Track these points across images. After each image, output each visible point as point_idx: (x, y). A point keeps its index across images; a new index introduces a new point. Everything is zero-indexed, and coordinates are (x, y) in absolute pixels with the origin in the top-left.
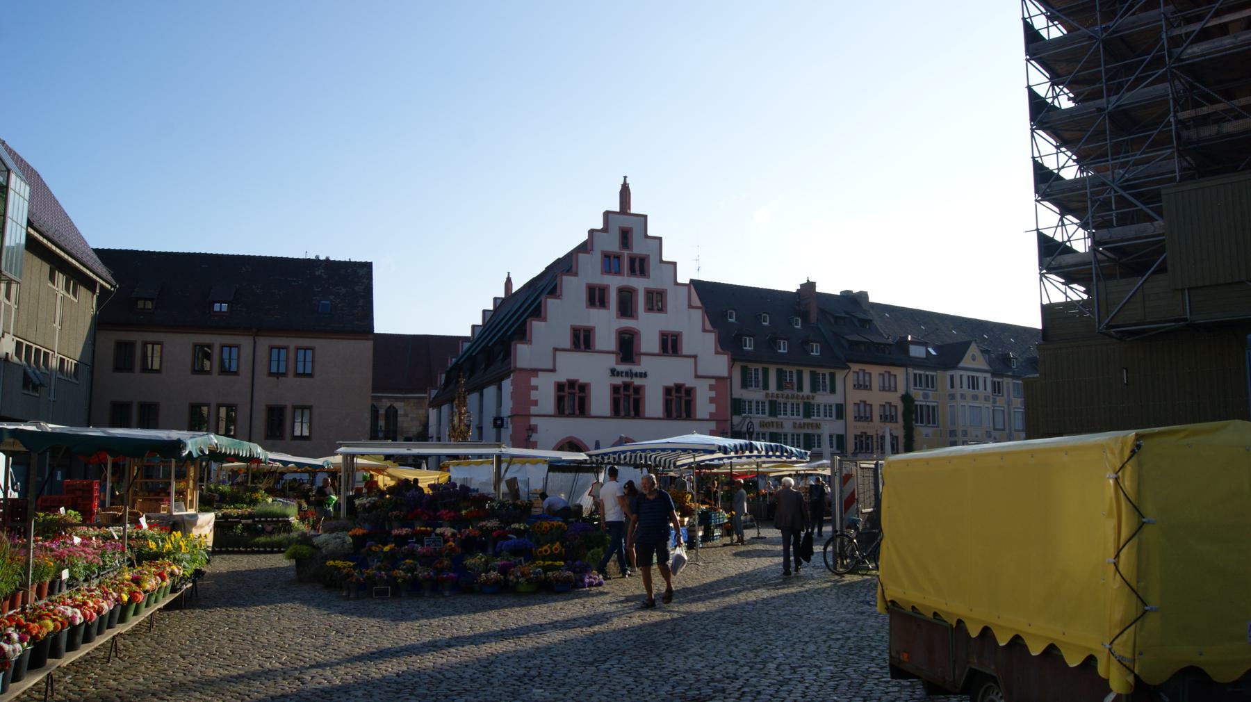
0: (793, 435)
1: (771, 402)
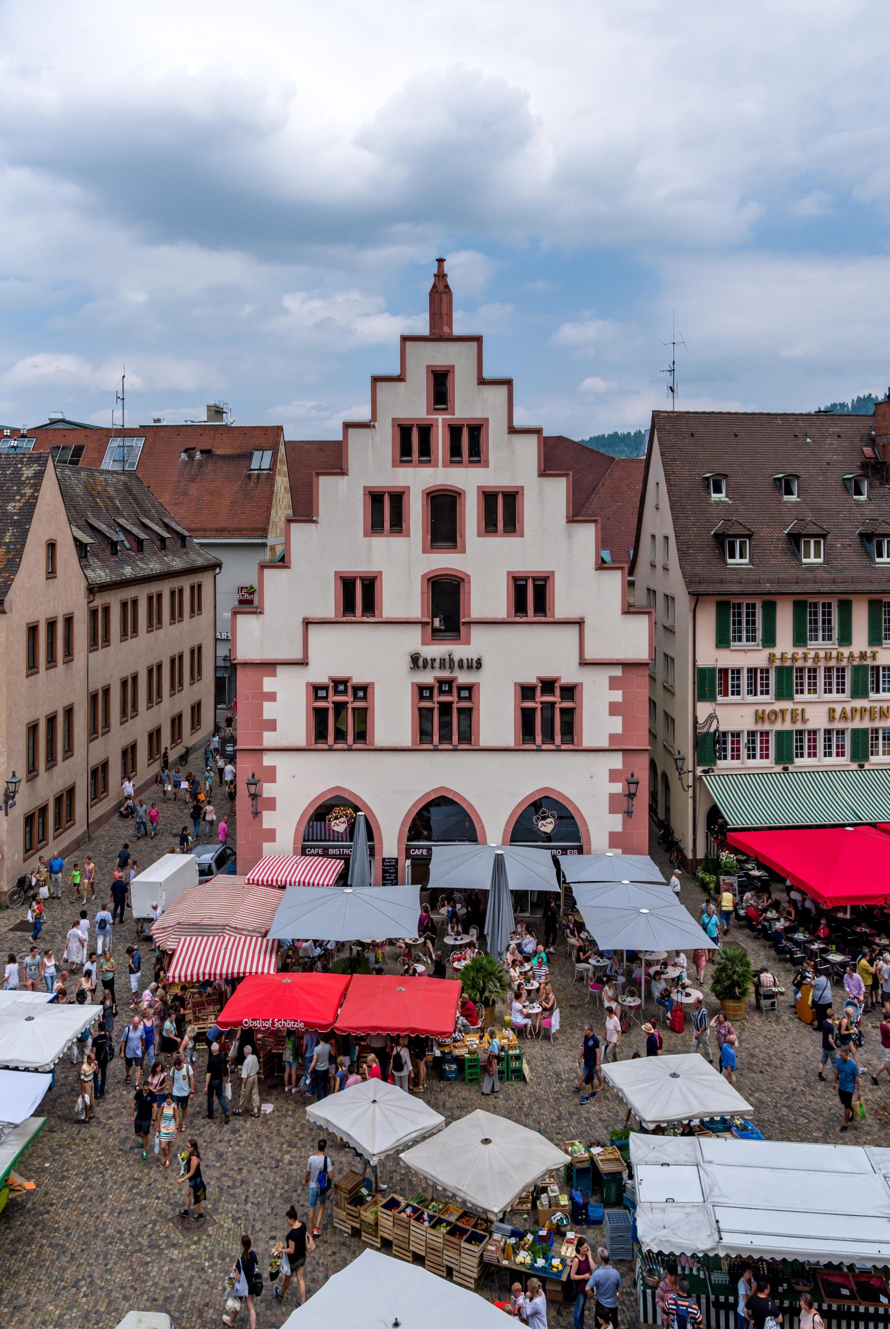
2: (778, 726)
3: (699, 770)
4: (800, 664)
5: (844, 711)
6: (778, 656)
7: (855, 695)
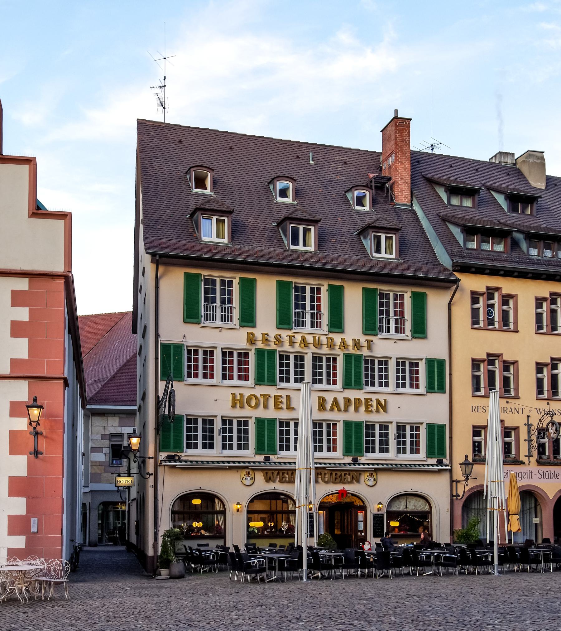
1: (260, 353)
2: (261, 413)
3: (162, 456)
4: (287, 347)
5: (335, 401)
7: (347, 385)
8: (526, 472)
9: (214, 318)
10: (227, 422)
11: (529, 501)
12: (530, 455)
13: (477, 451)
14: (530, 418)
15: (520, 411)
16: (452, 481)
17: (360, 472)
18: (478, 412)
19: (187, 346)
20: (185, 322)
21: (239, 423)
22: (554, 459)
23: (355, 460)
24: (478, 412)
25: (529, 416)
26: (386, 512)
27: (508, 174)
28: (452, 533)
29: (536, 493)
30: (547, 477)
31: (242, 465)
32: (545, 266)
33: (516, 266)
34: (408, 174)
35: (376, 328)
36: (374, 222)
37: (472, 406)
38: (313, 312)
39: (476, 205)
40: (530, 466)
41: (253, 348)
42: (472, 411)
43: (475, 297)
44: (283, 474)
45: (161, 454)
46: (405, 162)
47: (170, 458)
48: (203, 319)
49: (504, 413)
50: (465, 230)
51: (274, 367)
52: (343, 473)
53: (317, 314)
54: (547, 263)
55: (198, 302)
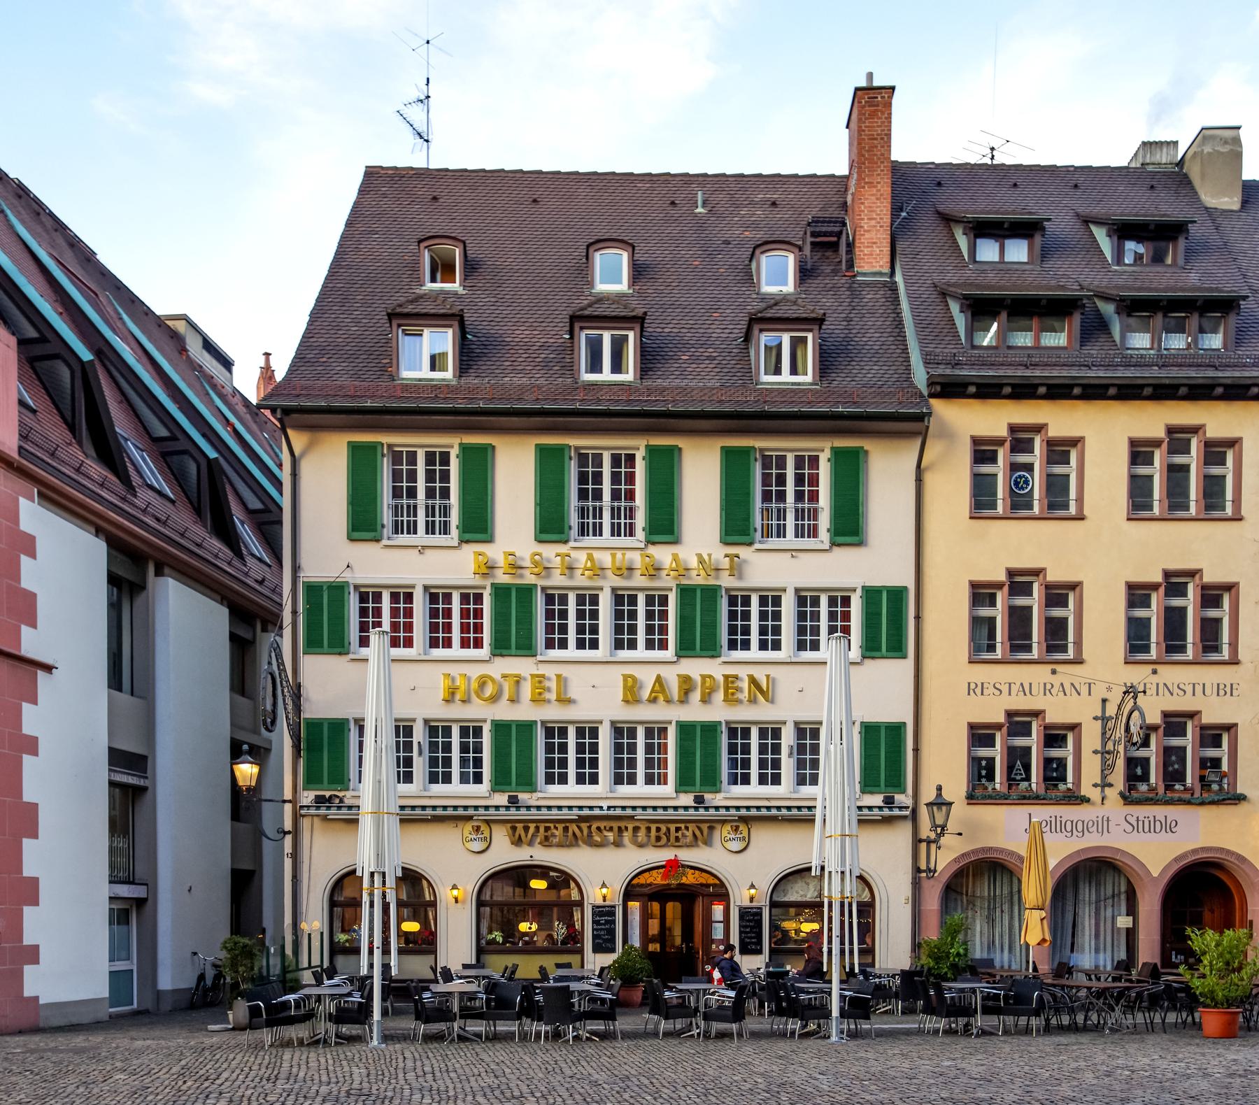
0: (617, 730)
2: (505, 712)
3: (308, 797)
4: (557, 580)
6: (501, 561)
7: (686, 648)
8: (1095, 819)
9: (781, 532)
10: (437, 730)
11: (1097, 878)
12: (1105, 785)
13: (984, 777)
14: (1107, 704)
15: (1084, 690)
16: (917, 841)
17: (712, 824)
18: (982, 694)
19: (727, 590)
20: (351, 539)
21: (464, 732)
22: (1166, 790)
23: (699, 800)
24: (982, 694)
25: (1104, 701)
26: (768, 903)
27: (1152, 187)
28: (916, 946)
29: (1120, 864)
30: (1147, 829)
31: (461, 812)
32: (1156, 368)
33: (1074, 373)
34: (884, 206)
35: (749, 529)
36: (766, 309)
37: (969, 684)
38: (782, 505)
39: (1043, 255)
40: (1105, 806)
41: (488, 583)
42: (969, 694)
43: (983, 452)
44: (547, 829)
45: (306, 793)
46: (879, 183)
47: (320, 800)
48: (759, 534)
49: (1045, 694)
50: (969, 306)
51: (531, 619)
52: (673, 827)
53: (408, 507)
54: (1165, 360)
55: (375, 498)
